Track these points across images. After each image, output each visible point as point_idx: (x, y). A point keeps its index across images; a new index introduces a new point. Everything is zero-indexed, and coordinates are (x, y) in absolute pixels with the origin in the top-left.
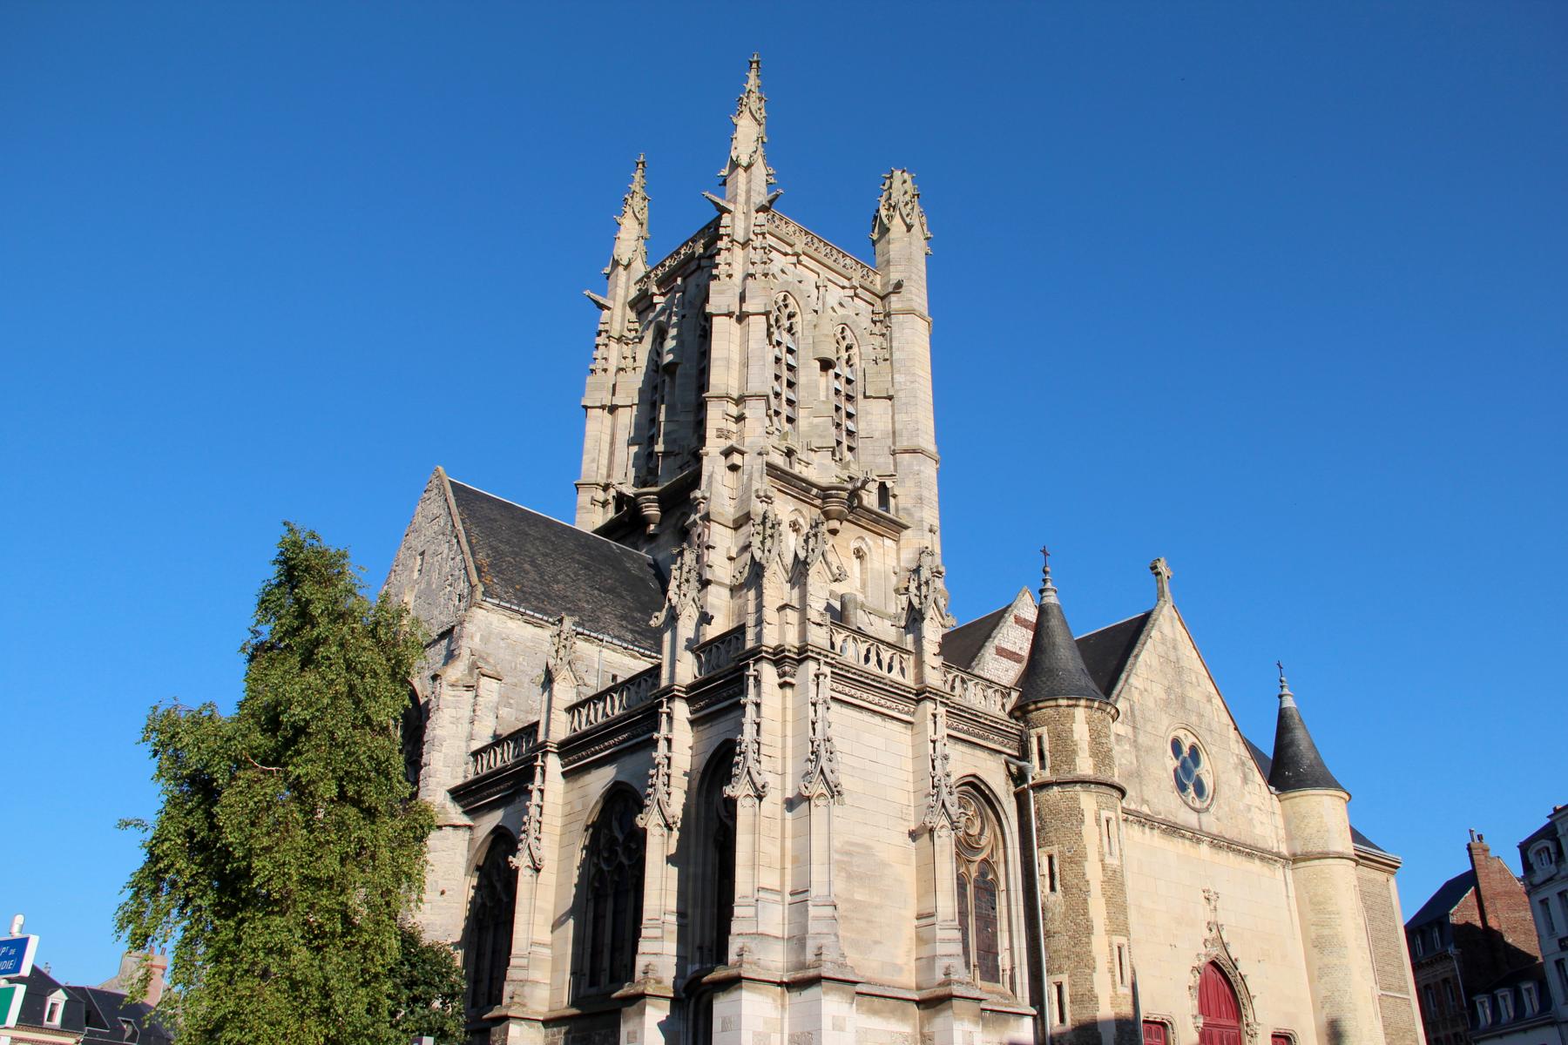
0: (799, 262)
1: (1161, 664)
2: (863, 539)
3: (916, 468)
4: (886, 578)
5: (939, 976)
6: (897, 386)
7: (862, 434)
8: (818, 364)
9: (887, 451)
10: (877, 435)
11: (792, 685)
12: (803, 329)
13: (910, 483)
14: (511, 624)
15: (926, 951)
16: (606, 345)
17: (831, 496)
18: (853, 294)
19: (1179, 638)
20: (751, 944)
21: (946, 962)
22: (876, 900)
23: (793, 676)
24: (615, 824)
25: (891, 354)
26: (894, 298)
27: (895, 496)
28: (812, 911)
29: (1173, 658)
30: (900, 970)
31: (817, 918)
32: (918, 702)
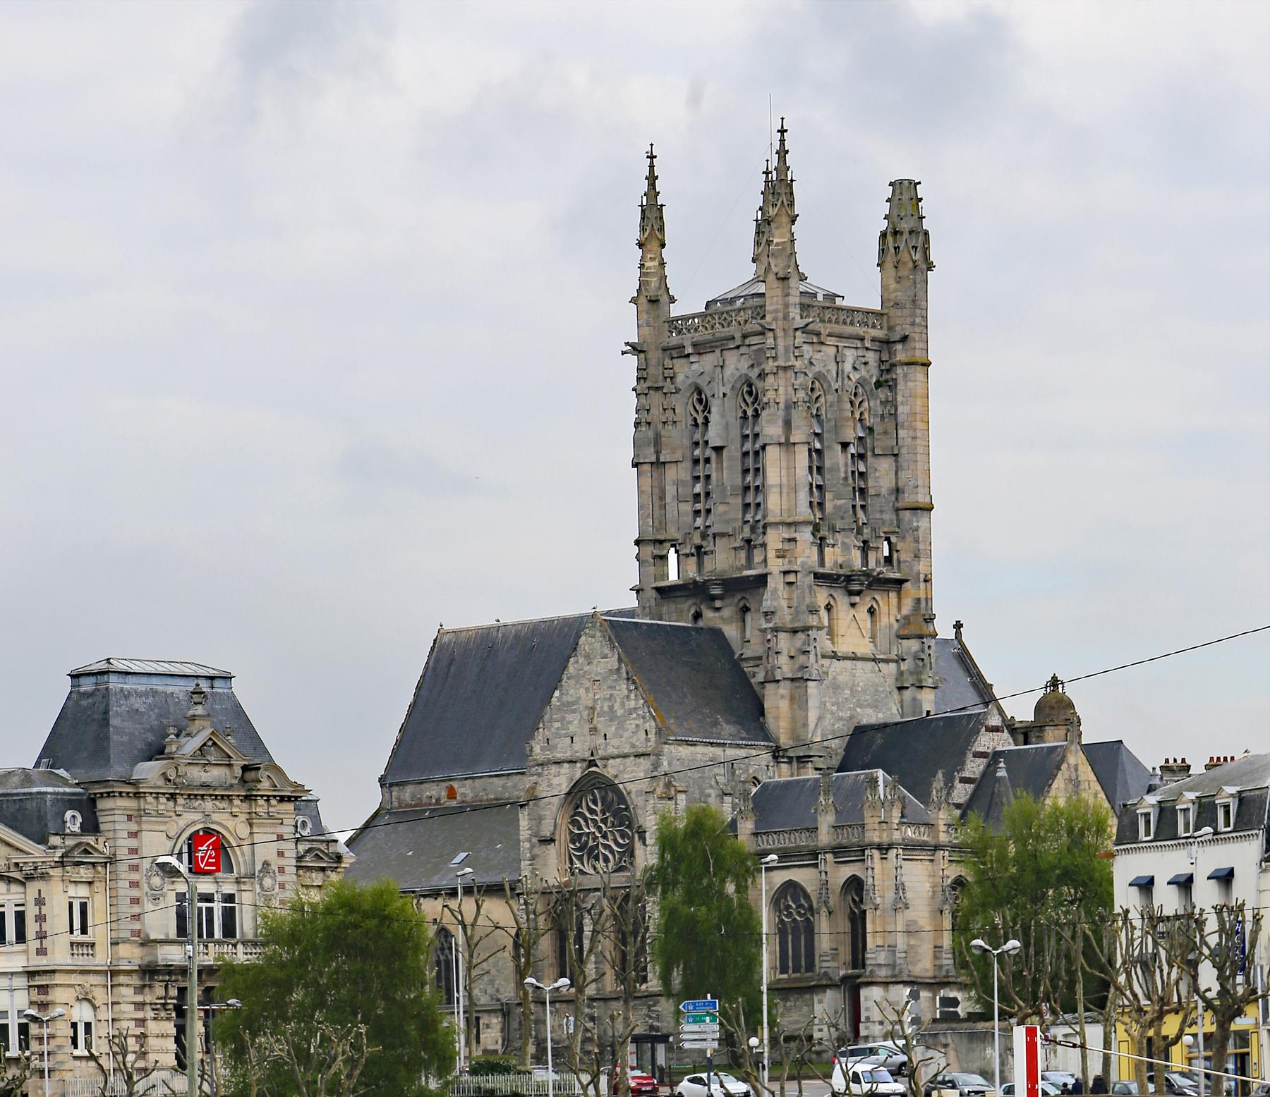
1: (1066, 784)
3: (915, 524)
5: (944, 973)
7: (871, 492)
8: (840, 446)
10: (884, 491)
11: (886, 858)
12: (826, 410)
13: (909, 539)
14: (680, 749)
15: (938, 963)
16: (646, 394)
17: (854, 580)
19: (1080, 763)
20: (876, 969)
22: (919, 943)
23: (886, 854)
24: (789, 898)
25: (896, 410)
26: (899, 347)
27: (897, 551)
28: (898, 955)
29: (1074, 777)
30: (927, 970)
31: (899, 958)
32: (935, 850)
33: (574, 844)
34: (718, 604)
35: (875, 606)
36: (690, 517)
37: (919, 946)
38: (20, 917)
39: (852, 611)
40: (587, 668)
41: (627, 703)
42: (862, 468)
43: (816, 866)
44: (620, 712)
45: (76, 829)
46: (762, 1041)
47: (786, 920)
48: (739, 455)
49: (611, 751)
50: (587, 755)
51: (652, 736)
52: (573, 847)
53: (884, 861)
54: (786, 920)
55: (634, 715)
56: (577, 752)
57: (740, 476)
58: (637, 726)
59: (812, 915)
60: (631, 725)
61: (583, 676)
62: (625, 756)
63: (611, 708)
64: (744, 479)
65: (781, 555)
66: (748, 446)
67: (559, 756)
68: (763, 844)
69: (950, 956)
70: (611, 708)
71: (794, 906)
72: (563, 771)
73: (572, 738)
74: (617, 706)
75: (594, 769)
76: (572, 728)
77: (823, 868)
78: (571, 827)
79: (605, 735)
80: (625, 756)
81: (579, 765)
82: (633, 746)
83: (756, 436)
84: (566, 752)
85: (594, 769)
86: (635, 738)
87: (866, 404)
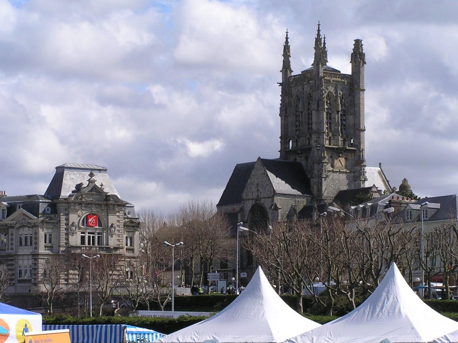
2: (347, 155)
7: (347, 125)
34: (300, 156)
38: (31, 237)
42: (344, 118)
45: (49, 212)
46: (236, 279)
48: (307, 114)
49: (262, 196)
63: (262, 184)
65: (316, 142)
70: (262, 184)
73: (253, 193)
74: (264, 184)
76: (253, 190)
82: (267, 195)
85: (257, 202)
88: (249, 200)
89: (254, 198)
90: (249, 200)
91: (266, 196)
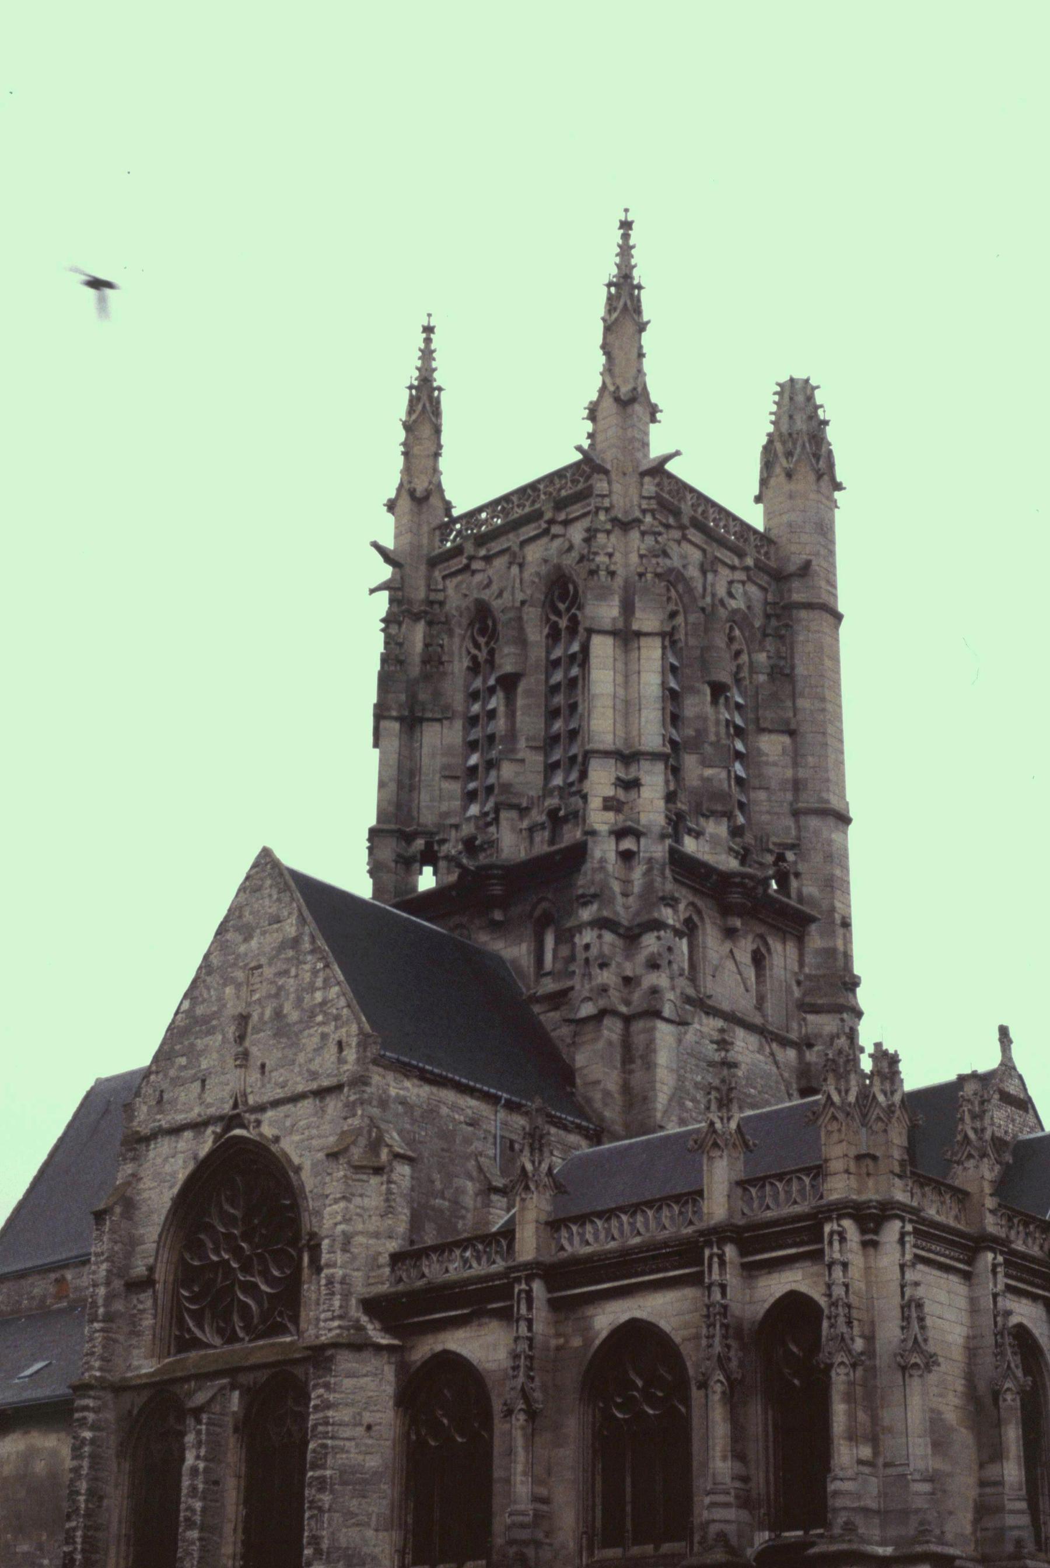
0: (684, 537)
4: (789, 991)
6: (799, 717)
9: (786, 808)
18: (744, 578)
20: (859, 1520)
21: (1016, 1533)
33: (189, 1288)
35: (763, 950)
36: (457, 804)
37: (950, 1475)
39: (728, 945)
40: (242, 949)
41: (307, 997)
43: (695, 1280)
44: (294, 1016)
47: (620, 1416)
50: (227, 1108)
51: (351, 1055)
52: (186, 1294)
53: (871, 1251)
54: (620, 1416)
55: (320, 1018)
56: (209, 1105)
57: (543, 720)
58: (324, 1036)
59: (686, 1401)
60: (310, 1040)
61: (235, 965)
62: (295, 1099)
63: (278, 1014)
64: (548, 725)
65: (610, 805)
66: (558, 677)
67: (181, 1118)
68: (571, 1244)
69: (1023, 1505)
70: (278, 1014)
71: (640, 1383)
72: (182, 1145)
73: (203, 1081)
74: (287, 1008)
75: (238, 1132)
77: (715, 1276)
78: (187, 1256)
79: (263, 1066)
80: (295, 1099)
81: (210, 1130)
82: (314, 1075)
83: (573, 734)
84: (192, 1109)
85: (238, 1132)
86: (318, 1060)
87: (744, 658)
88: (176, 1131)
89: (212, 1111)
90: (176, 1131)
91: (300, 1088)
